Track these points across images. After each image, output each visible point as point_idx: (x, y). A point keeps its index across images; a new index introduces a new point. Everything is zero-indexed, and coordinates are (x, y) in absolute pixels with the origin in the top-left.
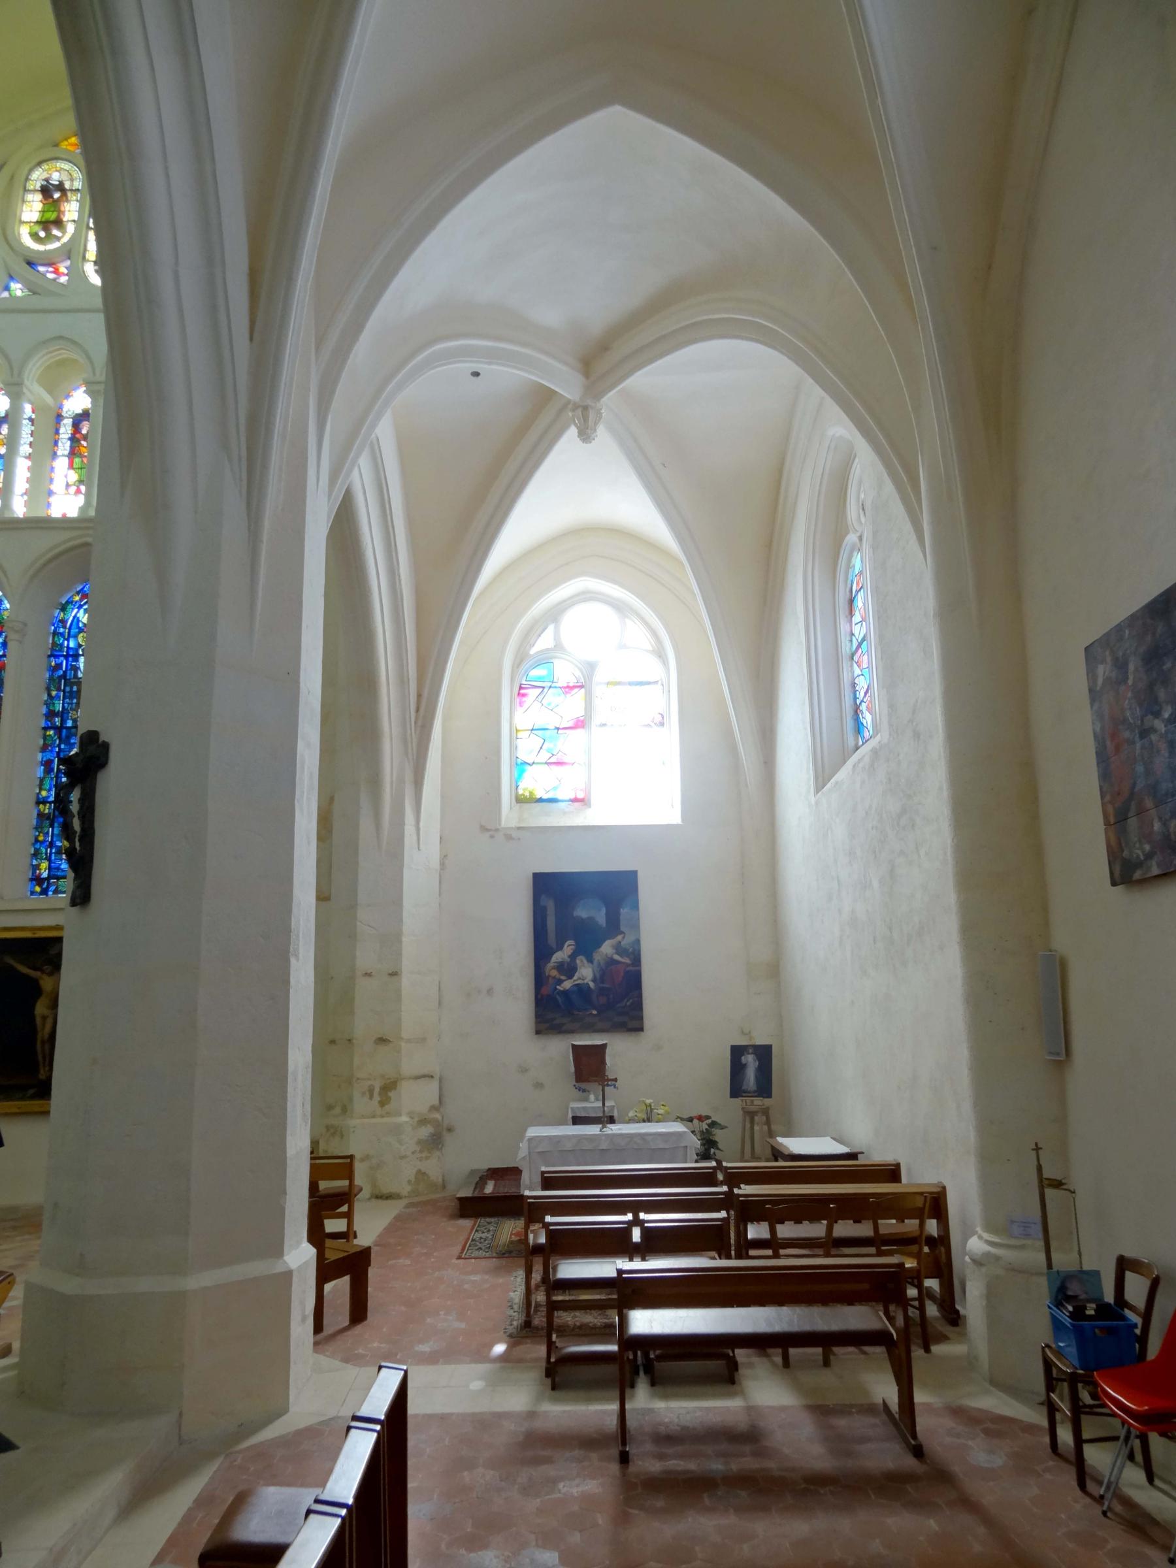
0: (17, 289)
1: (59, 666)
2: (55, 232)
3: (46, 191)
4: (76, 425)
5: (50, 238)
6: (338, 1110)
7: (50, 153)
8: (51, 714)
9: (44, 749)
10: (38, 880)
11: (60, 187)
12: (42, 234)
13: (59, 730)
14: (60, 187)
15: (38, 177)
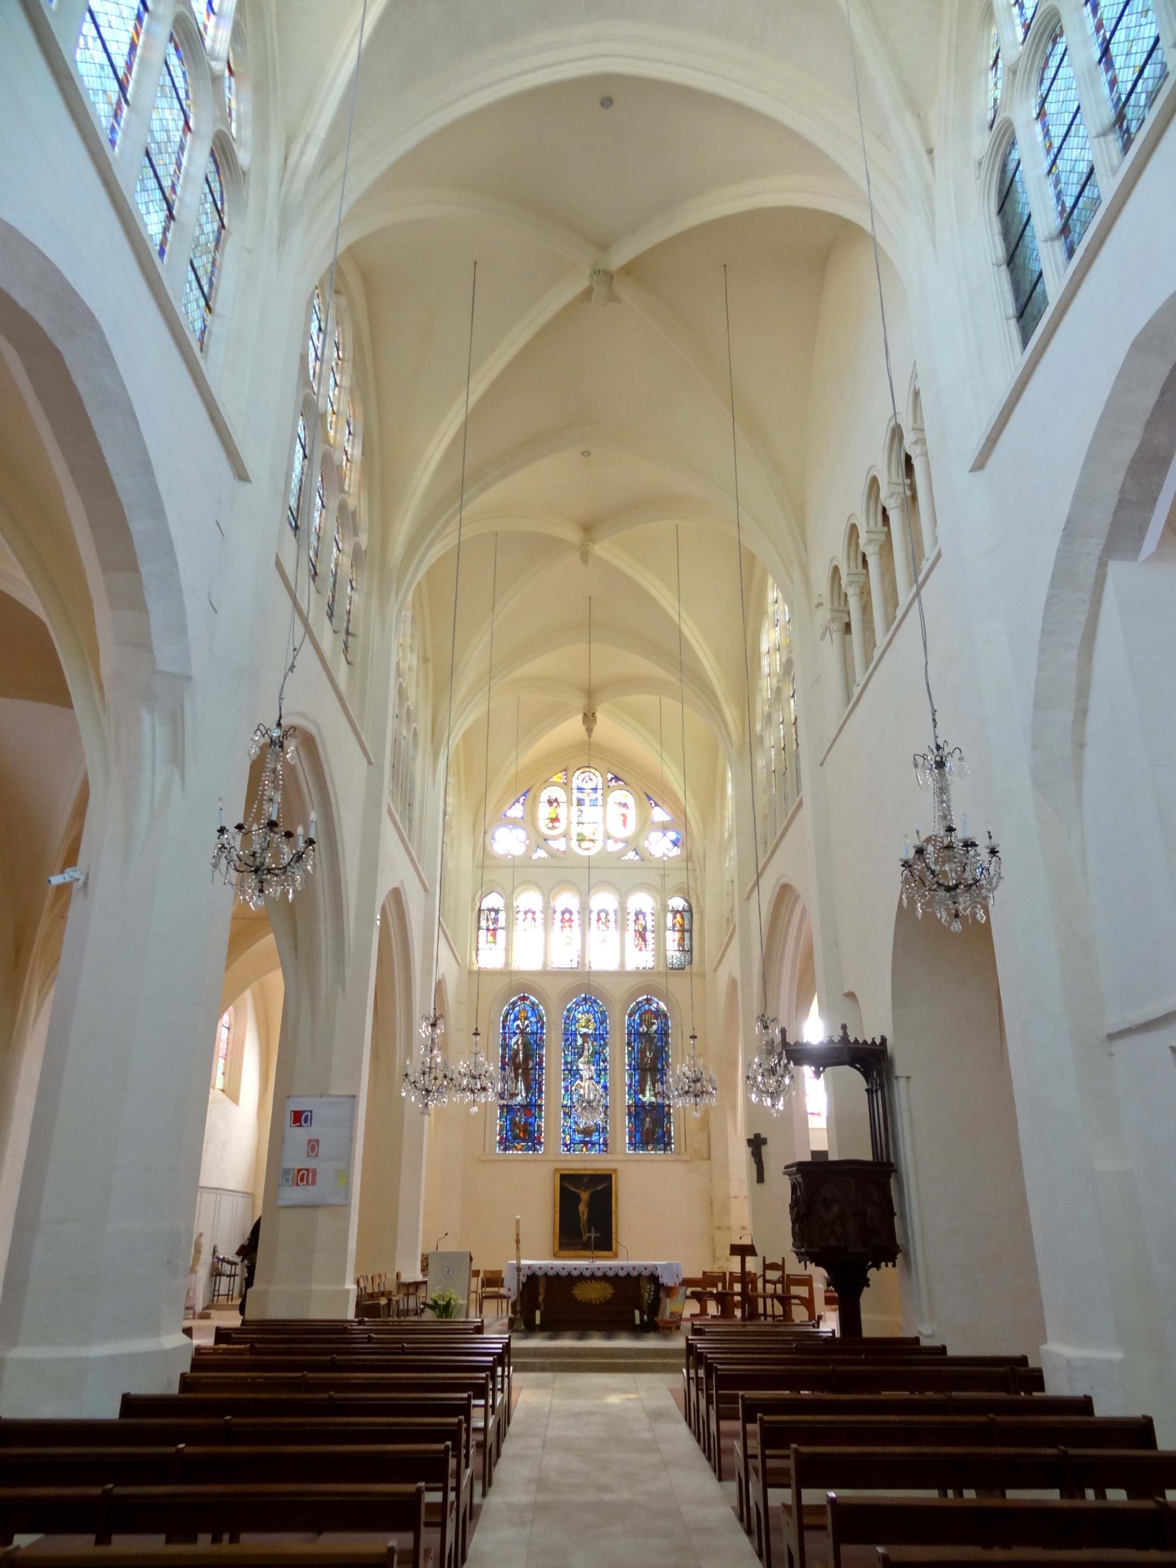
0: (541, 854)
1: (567, 1040)
2: (556, 824)
3: (550, 802)
4: (563, 913)
5: (553, 828)
6: (724, 1260)
7: (547, 783)
8: (566, 1063)
9: (564, 1079)
10: (565, 1145)
11: (556, 800)
12: (550, 825)
13: (570, 1071)
14: (556, 800)
15: (545, 795)
